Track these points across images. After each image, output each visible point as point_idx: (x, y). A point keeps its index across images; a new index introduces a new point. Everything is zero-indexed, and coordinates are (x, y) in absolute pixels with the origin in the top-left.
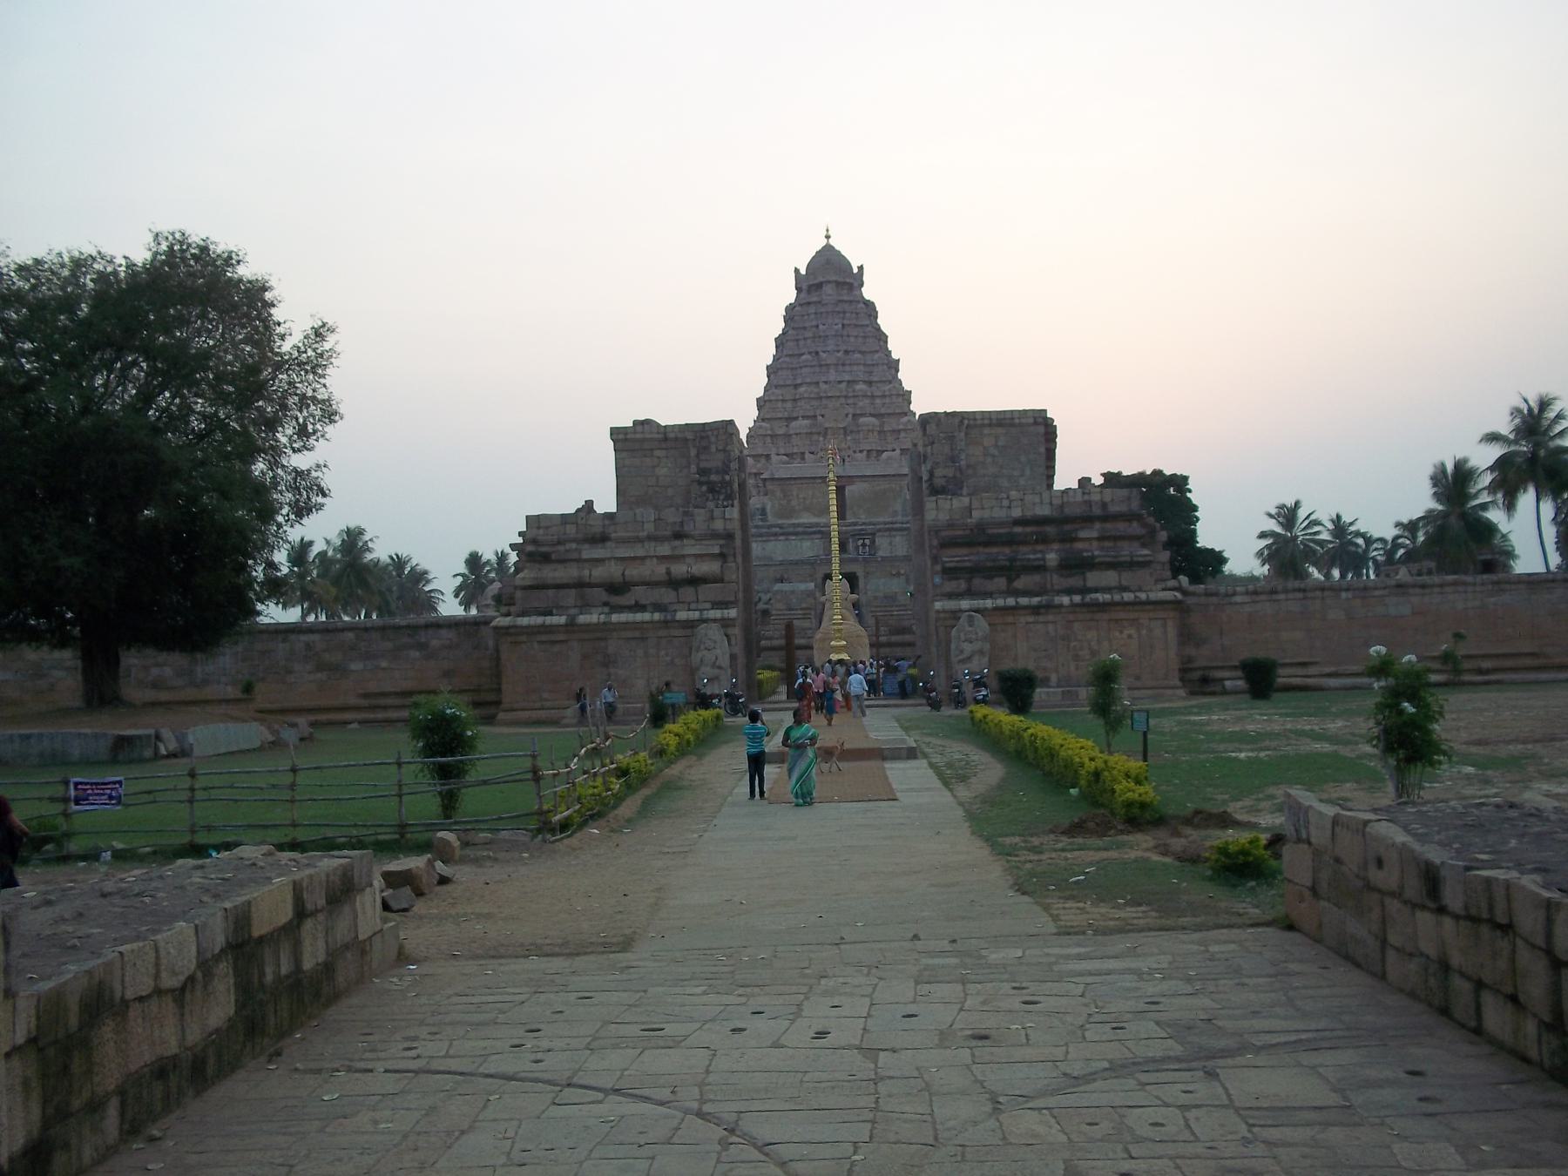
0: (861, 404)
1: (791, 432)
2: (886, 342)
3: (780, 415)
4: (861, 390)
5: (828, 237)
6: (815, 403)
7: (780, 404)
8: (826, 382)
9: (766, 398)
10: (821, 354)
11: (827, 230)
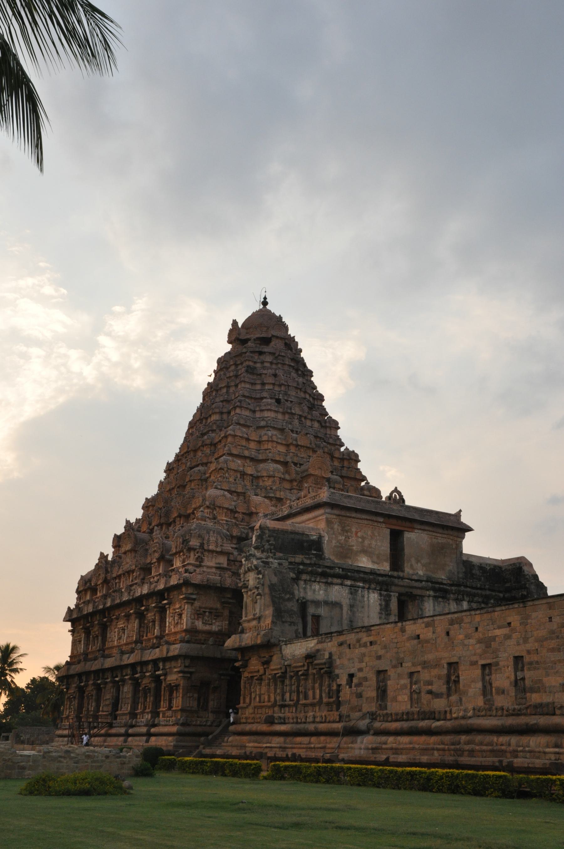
1: (259, 474)
3: (246, 453)
5: (265, 303)
7: (244, 443)
8: (292, 431)
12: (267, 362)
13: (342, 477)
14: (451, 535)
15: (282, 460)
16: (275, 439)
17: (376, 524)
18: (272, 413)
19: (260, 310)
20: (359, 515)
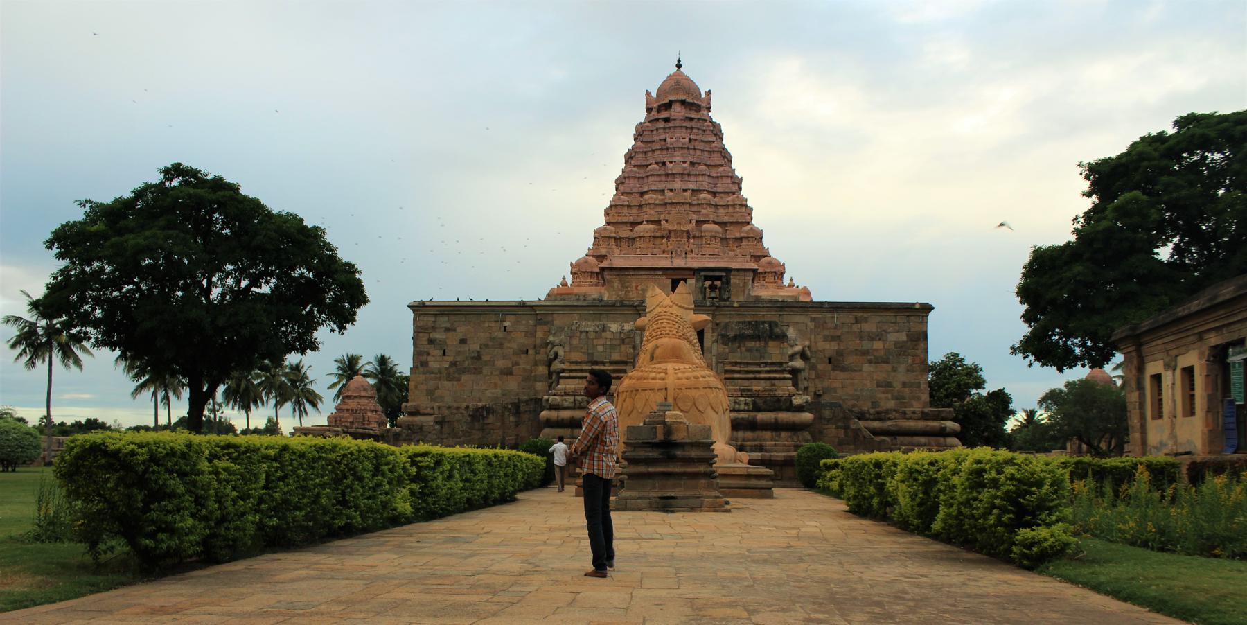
0: (704, 211)
1: (635, 236)
2: (730, 161)
3: (625, 220)
4: (704, 199)
5: (679, 66)
6: (659, 209)
7: (625, 210)
8: (671, 190)
9: (613, 203)
10: (668, 164)
11: (679, 61)
12: (661, 128)
13: (723, 224)
14: (738, 275)
15: (656, 219)
16: (651, 201)
17: (656, 277)
18: (655, 177)
19: (675, 74)
20: (637, 272)
